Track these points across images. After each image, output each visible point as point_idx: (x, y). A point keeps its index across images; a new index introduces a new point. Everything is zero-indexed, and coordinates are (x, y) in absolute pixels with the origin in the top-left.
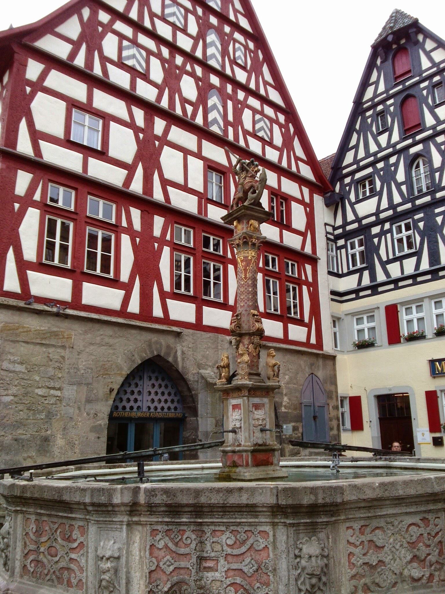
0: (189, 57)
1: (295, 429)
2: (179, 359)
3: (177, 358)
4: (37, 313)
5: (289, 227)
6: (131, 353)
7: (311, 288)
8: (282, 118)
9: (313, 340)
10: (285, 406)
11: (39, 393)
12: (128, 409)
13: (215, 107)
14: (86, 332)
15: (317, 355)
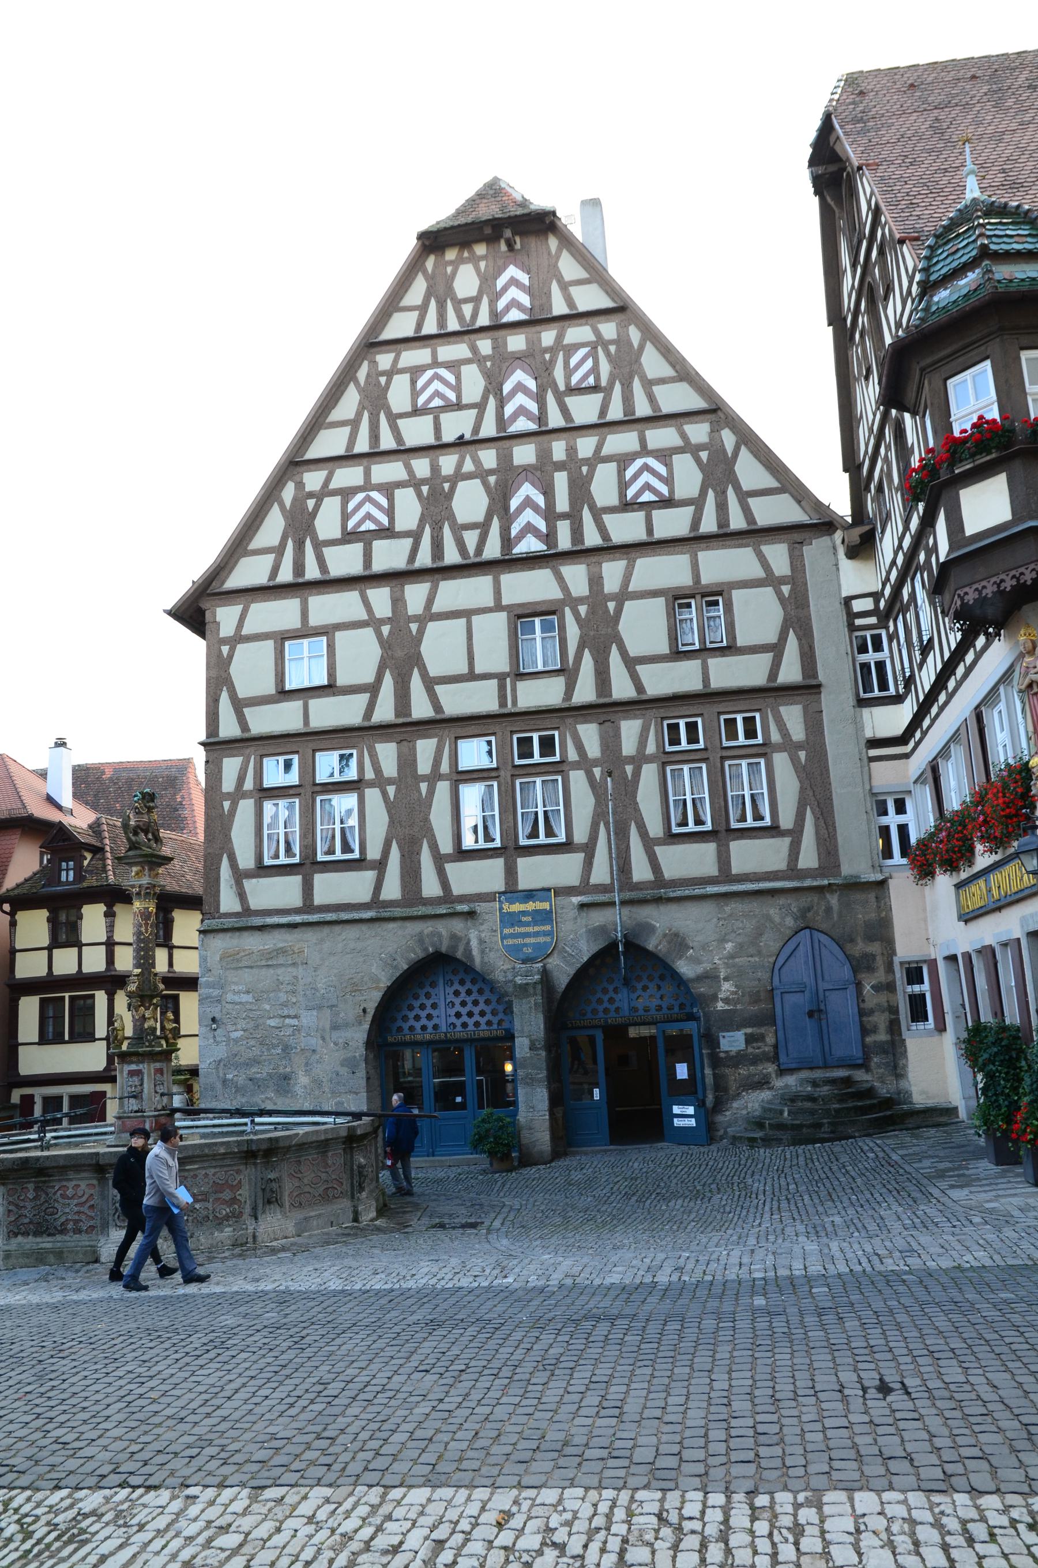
1: (750, 1039)
2: (475, 952)
3: (470, 951)
10: (726, 1001)
12: (419, 1030)
13: (528, 502)
14: (322, 941)
15: (820, 889)
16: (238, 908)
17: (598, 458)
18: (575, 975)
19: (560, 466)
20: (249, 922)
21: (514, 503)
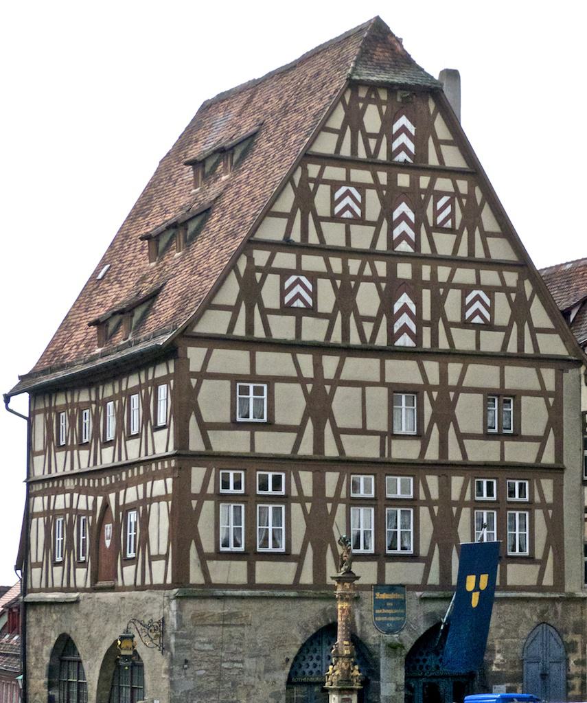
0: (369, 255)
1: (509, 690)
2: (358, 624)
3: (355, 622)
4: (218, 599)
5: (516, 436)
6: (305, 624)
7: (550, 512)
8: (511, 278)
9: (548, 581)
10: (498, 665)
11: (226, 667)
13: (405, 308)
14: (260, 610)
15: (554, 600)
16: (202, 581)
17: (450, 285)
18: (415, 643)
19: (426, 285)
20: (209, 591)
21: (397, 307)
